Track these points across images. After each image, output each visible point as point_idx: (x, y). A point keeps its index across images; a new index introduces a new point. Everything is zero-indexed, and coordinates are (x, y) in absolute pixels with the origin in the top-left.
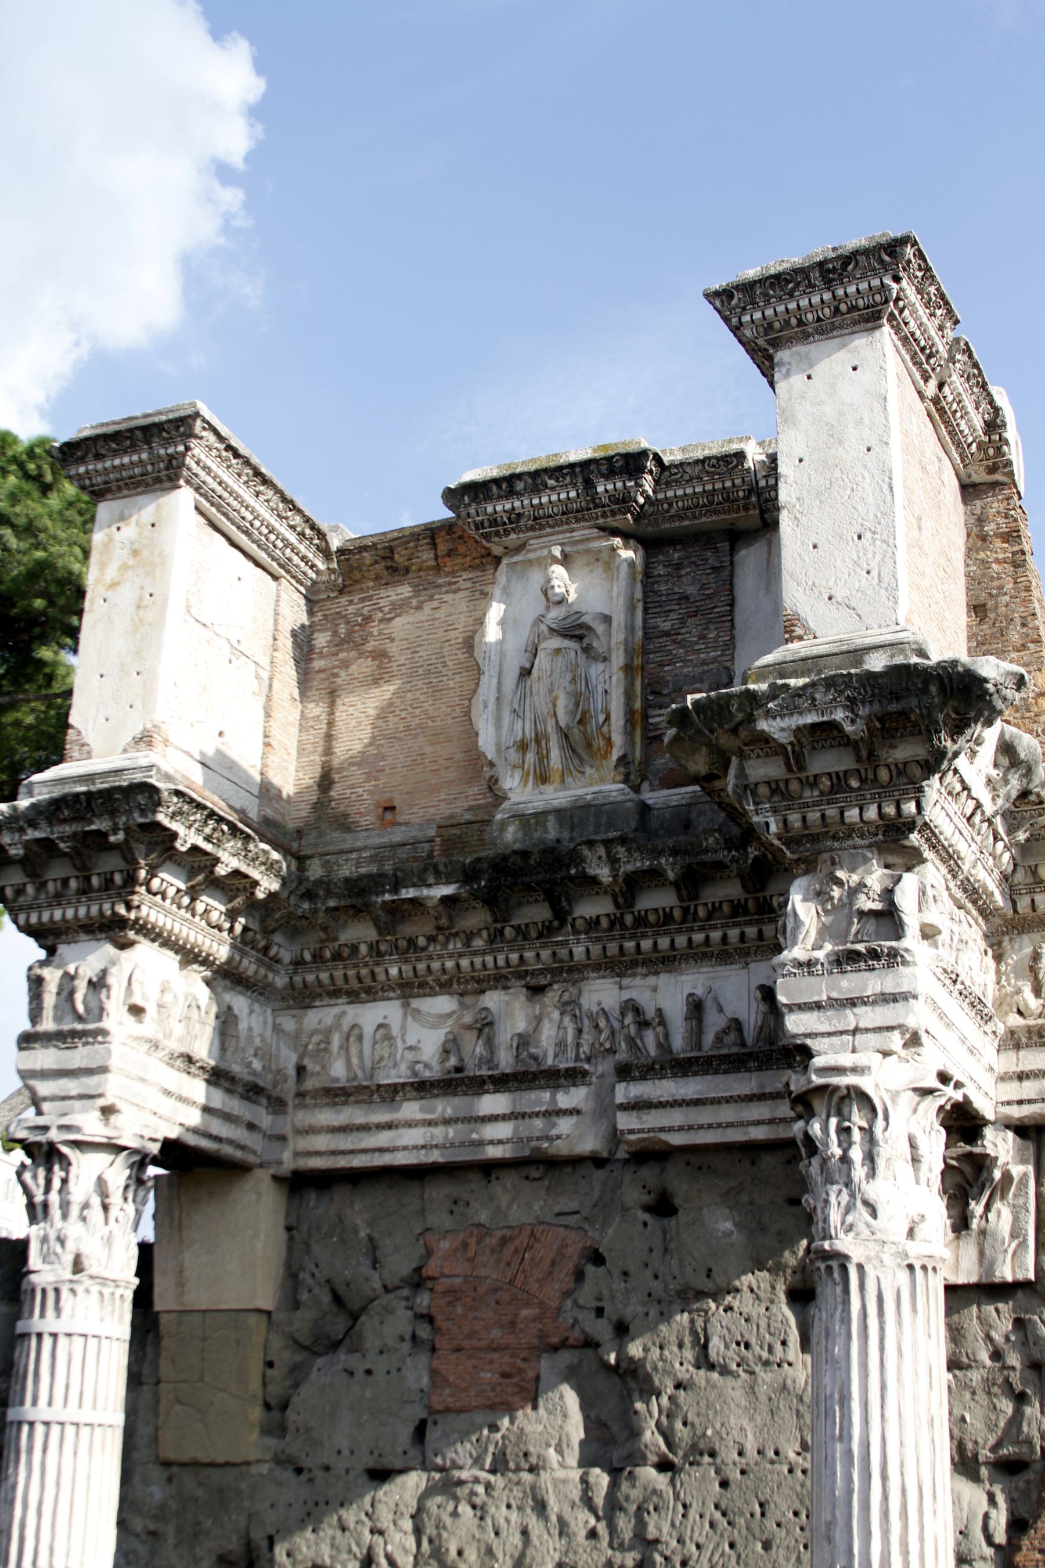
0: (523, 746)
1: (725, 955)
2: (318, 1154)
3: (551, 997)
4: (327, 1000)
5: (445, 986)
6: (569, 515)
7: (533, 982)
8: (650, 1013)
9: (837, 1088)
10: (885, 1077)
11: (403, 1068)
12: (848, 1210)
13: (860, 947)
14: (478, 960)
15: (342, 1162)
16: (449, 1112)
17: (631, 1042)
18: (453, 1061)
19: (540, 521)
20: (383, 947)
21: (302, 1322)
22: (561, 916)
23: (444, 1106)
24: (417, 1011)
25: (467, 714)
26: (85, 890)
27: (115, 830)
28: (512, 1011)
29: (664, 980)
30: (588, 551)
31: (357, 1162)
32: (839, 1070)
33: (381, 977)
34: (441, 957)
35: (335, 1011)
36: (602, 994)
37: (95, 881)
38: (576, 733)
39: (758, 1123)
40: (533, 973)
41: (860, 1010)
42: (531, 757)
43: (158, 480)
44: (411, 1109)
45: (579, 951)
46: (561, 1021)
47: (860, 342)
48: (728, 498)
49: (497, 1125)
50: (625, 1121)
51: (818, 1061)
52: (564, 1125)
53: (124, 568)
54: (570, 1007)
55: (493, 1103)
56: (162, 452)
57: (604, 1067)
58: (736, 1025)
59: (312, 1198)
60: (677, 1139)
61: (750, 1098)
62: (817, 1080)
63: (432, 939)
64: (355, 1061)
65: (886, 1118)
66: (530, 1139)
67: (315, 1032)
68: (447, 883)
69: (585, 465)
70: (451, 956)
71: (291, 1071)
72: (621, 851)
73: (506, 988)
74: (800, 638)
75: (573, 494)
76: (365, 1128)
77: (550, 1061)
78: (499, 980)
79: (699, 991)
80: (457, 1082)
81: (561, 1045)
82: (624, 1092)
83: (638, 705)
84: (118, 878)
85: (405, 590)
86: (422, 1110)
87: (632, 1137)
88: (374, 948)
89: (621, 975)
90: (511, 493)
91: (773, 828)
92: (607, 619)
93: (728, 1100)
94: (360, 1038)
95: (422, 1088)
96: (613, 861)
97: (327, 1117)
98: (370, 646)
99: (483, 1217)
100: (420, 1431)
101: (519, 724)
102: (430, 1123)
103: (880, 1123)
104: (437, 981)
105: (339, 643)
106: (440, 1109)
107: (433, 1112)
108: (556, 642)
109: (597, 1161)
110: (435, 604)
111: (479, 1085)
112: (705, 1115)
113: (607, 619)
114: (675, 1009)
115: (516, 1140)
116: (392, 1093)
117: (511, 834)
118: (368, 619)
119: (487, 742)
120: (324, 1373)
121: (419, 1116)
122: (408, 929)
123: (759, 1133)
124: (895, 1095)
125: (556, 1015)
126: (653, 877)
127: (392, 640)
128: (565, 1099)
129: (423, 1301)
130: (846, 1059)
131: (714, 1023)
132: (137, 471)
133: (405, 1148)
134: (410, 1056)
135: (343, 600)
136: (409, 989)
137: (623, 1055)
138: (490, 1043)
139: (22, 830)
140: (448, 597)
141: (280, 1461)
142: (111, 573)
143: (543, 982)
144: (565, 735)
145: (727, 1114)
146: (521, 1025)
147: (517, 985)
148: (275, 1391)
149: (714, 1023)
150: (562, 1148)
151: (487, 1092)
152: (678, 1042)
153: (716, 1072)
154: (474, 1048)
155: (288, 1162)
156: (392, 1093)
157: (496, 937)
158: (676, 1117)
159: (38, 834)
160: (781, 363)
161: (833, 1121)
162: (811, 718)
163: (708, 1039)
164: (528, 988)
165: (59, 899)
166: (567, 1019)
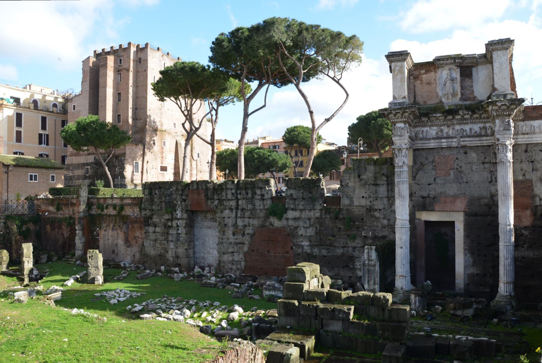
0: (445, 95)
1: (475, 123)
5: (436, 126)
6: (451, 64)
10: (508, 143)
17: (462, 134)
19: (447, 64)
21: (417, 167)
23: (437, 141)
25: (436, 89)
26: (402, 117)
28: (445, 129)
29: (466, 126)
36: (457, 127)
44: (432, 141)
45: (455, 122)
48: (473, 62)
49: (444, 143)
50: (462, 143)
52: (454, 143)
55: (443, 140)
57: (459, 136)
58: (476, 132)
59: (417, 151)
69: (455, 58)
78: (444, 125)
81: (453, 134)
82: (461, 139)
88: (427, 121)
90: (443, 60)
92: (456, 78)
95: (434, 139)
96: (463, 112)
97: (420, 142)
99: (442, 154)
100: (435, 179)
108: (450, 82)
109: (456, 147)
111: (442, 138)
113: (456, 78)
114: (468, 130)
116: (429, 139)
117: (447, 108)
119: (440, 94)
120: (420, 173)
122: (432, 119)
123: (479, 145)
126: (468, 114)
128: (453, 140)
129: (434, 164)
131: (473, 132)
136: (430, 126)
137: (461, 134)
141: (415, 183)
145: (475, 142)
148: (414, 175)
149: (473, 132)
150: (453, 146)
154: (440, 134)
155: (415, 148)
156: (429, 139)
157: (444, 120)
158: (469, 143)
163: (473, 133)
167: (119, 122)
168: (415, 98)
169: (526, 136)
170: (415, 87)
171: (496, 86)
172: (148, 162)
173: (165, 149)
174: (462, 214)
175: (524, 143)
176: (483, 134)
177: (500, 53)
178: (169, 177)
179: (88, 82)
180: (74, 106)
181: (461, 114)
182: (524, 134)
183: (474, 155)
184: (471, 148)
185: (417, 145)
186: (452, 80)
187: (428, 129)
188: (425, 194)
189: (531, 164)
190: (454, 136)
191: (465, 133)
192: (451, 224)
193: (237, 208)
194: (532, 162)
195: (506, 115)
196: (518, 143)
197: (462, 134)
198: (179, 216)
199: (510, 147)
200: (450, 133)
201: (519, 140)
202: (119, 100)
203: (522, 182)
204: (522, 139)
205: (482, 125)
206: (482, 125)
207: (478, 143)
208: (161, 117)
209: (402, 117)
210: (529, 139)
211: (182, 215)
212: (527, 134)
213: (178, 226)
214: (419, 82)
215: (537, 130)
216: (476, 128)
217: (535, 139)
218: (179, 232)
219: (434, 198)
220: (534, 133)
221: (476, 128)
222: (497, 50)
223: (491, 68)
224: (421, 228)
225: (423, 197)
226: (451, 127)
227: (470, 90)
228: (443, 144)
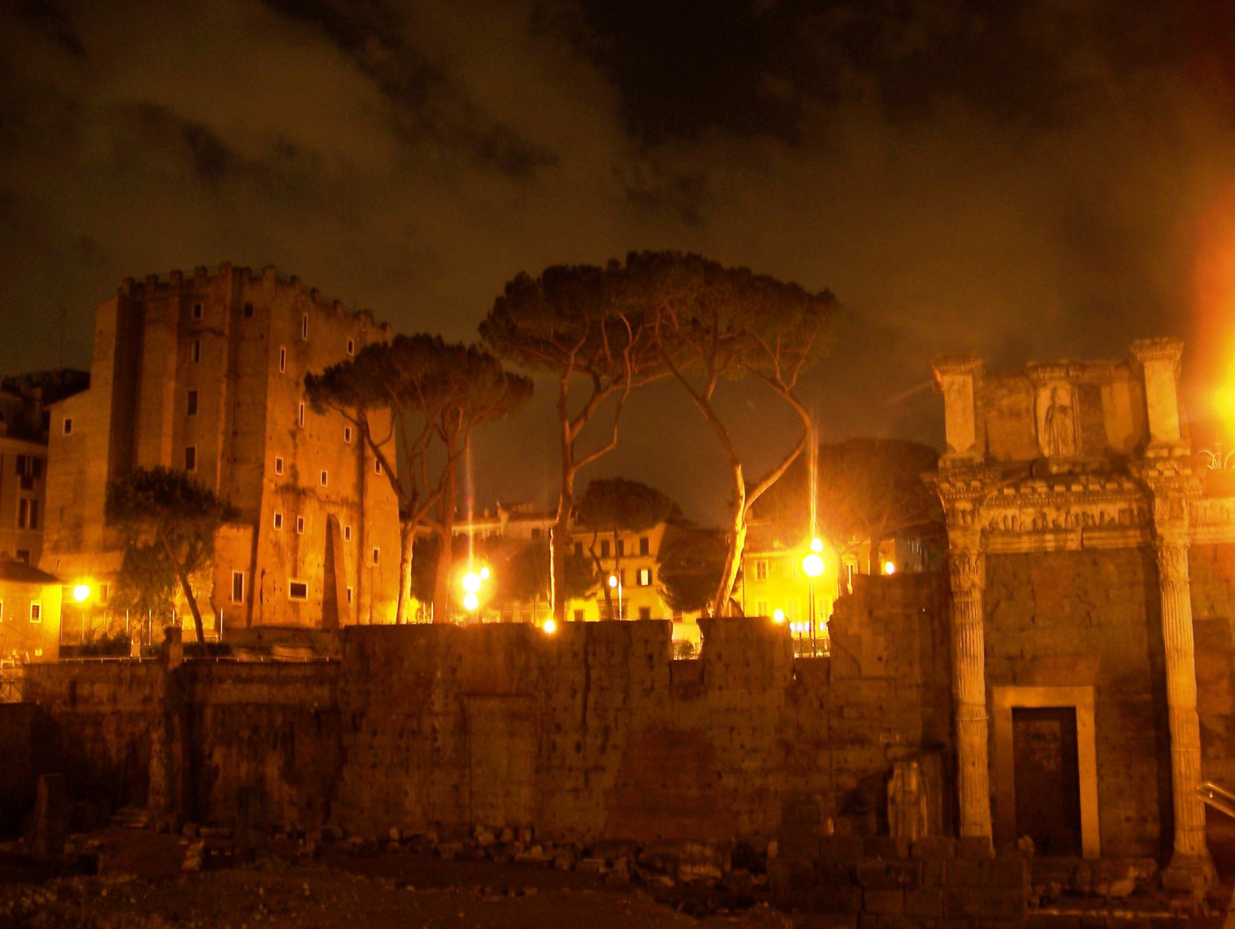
5: (1033, 505)
6: (1060, 378)
19: (1051, 379)
22: (1068, 489)
28: (1051, 514)
36: (1076, 509)
44: (1025, 538)
49: (1050, 542)
55: (1049, 537)
80: (1038, 531)
85: (1005, 392)
95: (1029, 533)
97: (1000, 540)
100: (1033, 619)
116: (1019, 535)
131: (1107, 518)
145: (1113, 541)
149: (1107, 518)
152: (1097, 522)
167: (190, 464)
170: (986, 423)
172: (263, 573)
173: (301, 540)
174: (1090, 690)
177: (1157, 365)
178: (310, 613)
179: (111, 363)
180: (68, 423)
183: (1111, 567)
184: (1104, 553)
186: (1063, 409)
188: (1013, 649)
191: (1090, 522)
192: (1067, 715)
193: (587, 689)
198: (437, 708)
199: (1184, 554)
200: (1062, 520)
202: (192, 409)
203: (1208, 623)
207: (1120, 543)
208: (294, 455)
211: (447, 705)
213: (434, 730)
216: (1112, 510)
218: (439, 744)
219: (1034, 659)
223: (1139, 391)
224: (1006, 727)
225: (1010, 658)
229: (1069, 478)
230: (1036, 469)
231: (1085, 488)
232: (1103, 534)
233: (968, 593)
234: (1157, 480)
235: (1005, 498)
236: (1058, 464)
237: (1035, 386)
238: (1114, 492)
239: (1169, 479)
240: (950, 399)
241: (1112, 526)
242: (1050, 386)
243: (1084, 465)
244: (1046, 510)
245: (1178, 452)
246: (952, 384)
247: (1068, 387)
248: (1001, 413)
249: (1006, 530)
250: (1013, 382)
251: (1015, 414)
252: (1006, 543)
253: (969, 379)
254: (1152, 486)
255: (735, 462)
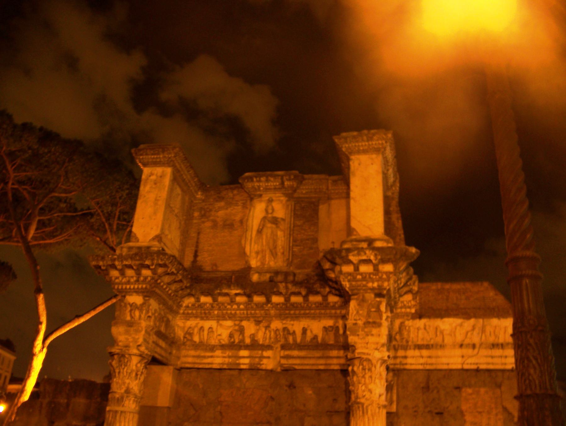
2: (189, 363)
3: (261, 325)
4: (193, 319)
5: (231, 317)
7: (257, 319)
8: (291, 332)
9: (363, 358)
11: (217, 341)
12: (364, 391)
13: (371, 320)
14: (242, 312)
15: (196, 366)
16: (230, 354)
18: (232, 340)
19: (267, 189)
20: (215, 305)
23: (228, 353)
24: (221, 325)
25: (240, 242)
27: (152, 265)
28: (250, 328)
29: (296, 323)
30: (279, 200)
31: (201, 366)
32: (364, 353)
33: (212, 314)
34: (230, 310)
35: (196, 322)
36: (276, 324)
37: (142, 278)
38: (273, 251)
39: (321, 365)
40: (258, 317)
41: (370, 337)
42: (260, 256)
43: (164, 164)
44: (218, 353)
46: (265, 331)
47: (374, 156)
49: (245, 359)
50: (283, 361)
51: (357, 351)
53: (151, 187)
54: (267, 327)
56: (167, 156)
57: (278, 345)
60: (297, 367)
61: (319, 358)
62: (357, 356)
63: (229, 304)
64: (202, 337)
65: (375, 367)
66: (254, 364)
67: (190, 328)
68: (237, 290)
70: (234, 310)
71: (182, 338)
72: (290, 286)
73: (249, 320)
74: (355, 235)
75: (278, 184)
76: (204, 357)
77: (261, 343)
79: (306, 326)
80: (232, 346)
81: (264, 338)
82: (283, 353)
83: (291, 245)
84: (149, 278)
85: (222, 204)
86: (222, 353)
87: (285, 366)
89: (283, 320)
91: (348, 286)
93: (313, 358)
94: (203, 331)
95: (223, 347)
96: (287, 288)
97: (192, 353)
98: (211, 218)
101: (256, 246)
102: (224, 357)
103: (373, 369)
104: (229, 317)
105: (203, 216)
106: (227, 353)
107: (225, 353)
110: (232, 208)
112: (306, 361)
115: (250, 364)
116: (212, 348)
118: (211, 210)
121: (221, 355)
123: (322, 367)
124: (377, 362)
125: (264, 330)
126: (299, 294)
127: (218, 217)
128: (265, 354)
130: (365, 351)
131: (309, 335)
132: (158, 160)
133: (216, 364)
134: (219, 337)
135: (204, 204)
137: (282, 341)
138: (243, 336)
139: (122, 261)
140: (236, 207)
142: (148, 188)
143: (260, 319)
144: (271, 251)
145: (312, 361)
146: (253, 331)
147: (252, 319)
149: (309, 335)
150: (263, 367)
151: (242, 349)
152: (299, 340)
153: (310, 349)
156: (212, 348)
158: (298, 361)
159: (127, 263)
160: (352, 159)
161: (361, 367)
162: (364, 258)
164: (255, 321)
165: (128, 282)
166: (267, 331)
168: (196, 256)
169: (425, 352)
170: (199, 234)
171: (353, 224)
175: (421, 367)
176: (332, 342)
177: (363, 158)
181: (283, 291)
182: (419, 347)
184: (304, 374)
185: (184, 360)
187: (212, 323)
189: (437, 418)
190: (267, 342)
191: (291, 339)
194: (440, 414)
195: (373, 289)
196: (408, 367)
197: (286, 339)
201: (409, 361)
204: (415, 360)
205: (330, 323)
206: (330, 323)
207: (321, 364)
209: (137, 281)
210: (430, 361)
212: (427, 347)
214: (208, 224)
215: (448, 340)
216: (316, 327)
217: (444, 360)
220: (442, 346)
221: (316, 327)
222: (359, 152)
226: (264, 324)
227: (311, 248)
228: (242, 361)
229: (268, 288)
230: (240, 278)
231: (287, 300)
232: (303, 353)
233: (120, 401)
234: (352, 277)
235: (201, 306)
236: (260, 273)
237: (252, 197)
238: (319, 306)
239: (366, 277)
240: (145, 189)
241: (315, 345)
242: (266, 197)
243: (286, 274)
244: (244, 323)
245: (378, 244)
246: (152, 174)
247: (284, 199)
248: (215, 225)
249: (201, 342)
250: (231, 195)
251: (229, 225)
252: (198, 357)
253: (169, 171)
254: (346, 284)
255: (39, 291)
